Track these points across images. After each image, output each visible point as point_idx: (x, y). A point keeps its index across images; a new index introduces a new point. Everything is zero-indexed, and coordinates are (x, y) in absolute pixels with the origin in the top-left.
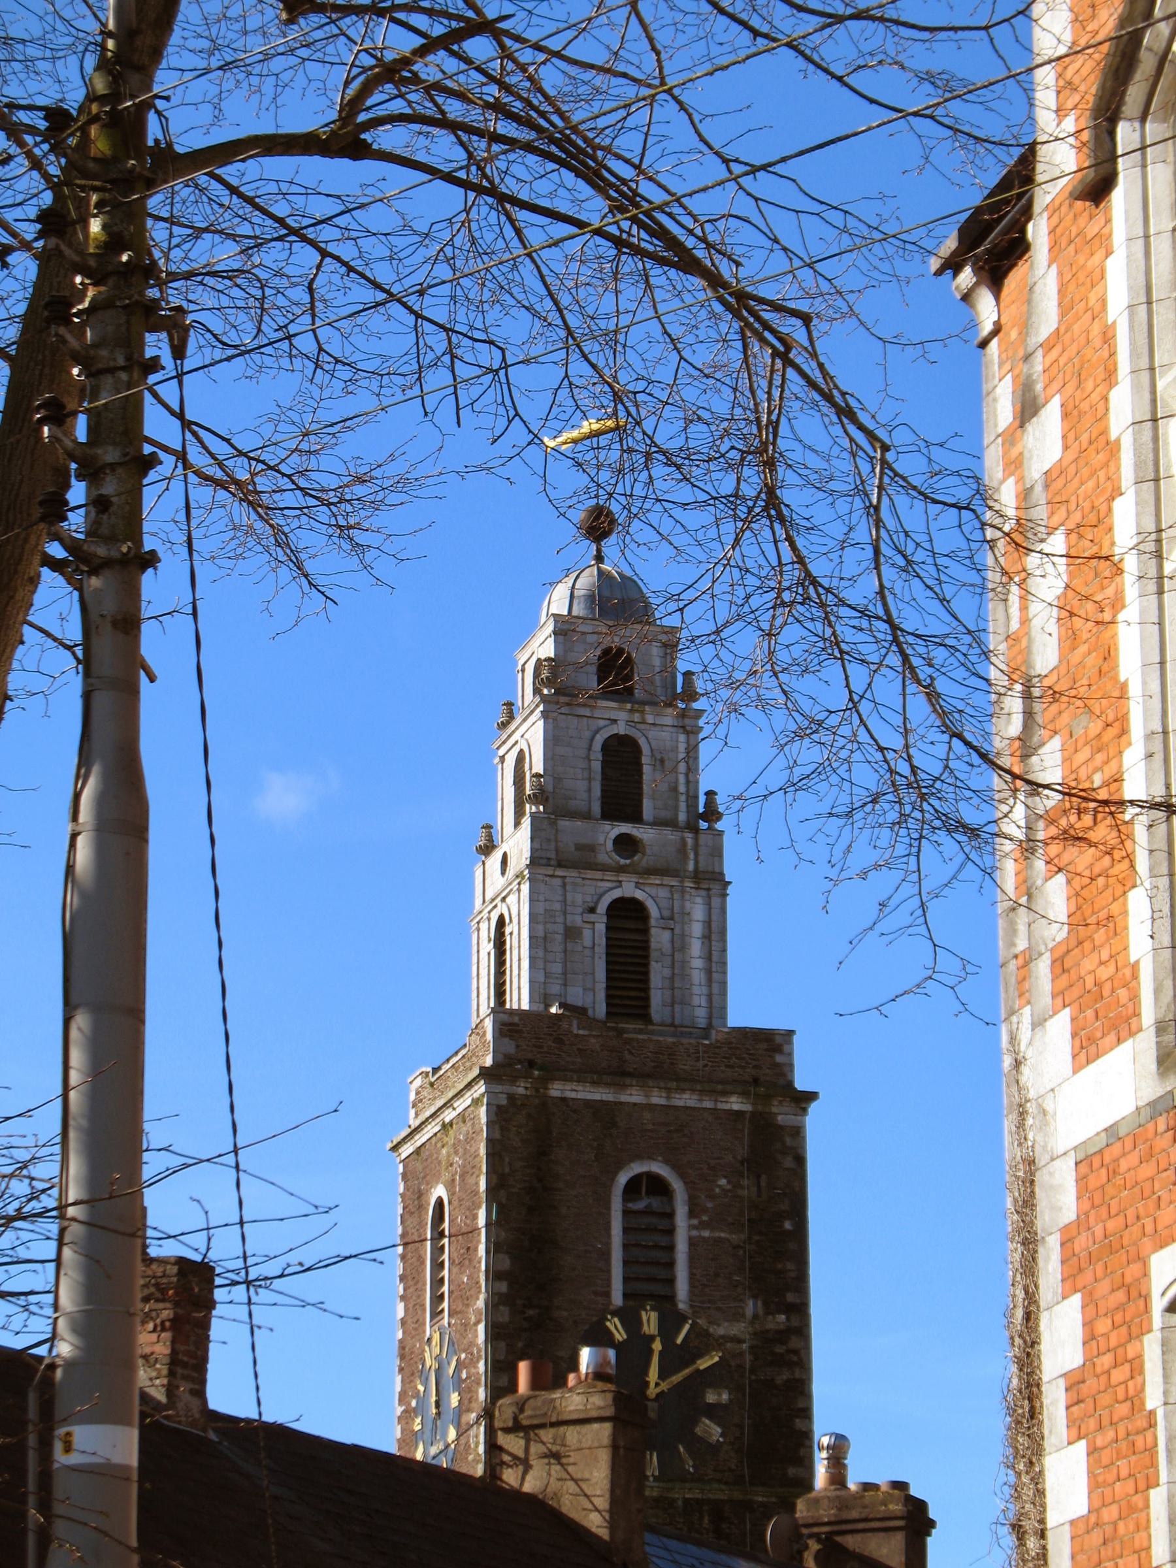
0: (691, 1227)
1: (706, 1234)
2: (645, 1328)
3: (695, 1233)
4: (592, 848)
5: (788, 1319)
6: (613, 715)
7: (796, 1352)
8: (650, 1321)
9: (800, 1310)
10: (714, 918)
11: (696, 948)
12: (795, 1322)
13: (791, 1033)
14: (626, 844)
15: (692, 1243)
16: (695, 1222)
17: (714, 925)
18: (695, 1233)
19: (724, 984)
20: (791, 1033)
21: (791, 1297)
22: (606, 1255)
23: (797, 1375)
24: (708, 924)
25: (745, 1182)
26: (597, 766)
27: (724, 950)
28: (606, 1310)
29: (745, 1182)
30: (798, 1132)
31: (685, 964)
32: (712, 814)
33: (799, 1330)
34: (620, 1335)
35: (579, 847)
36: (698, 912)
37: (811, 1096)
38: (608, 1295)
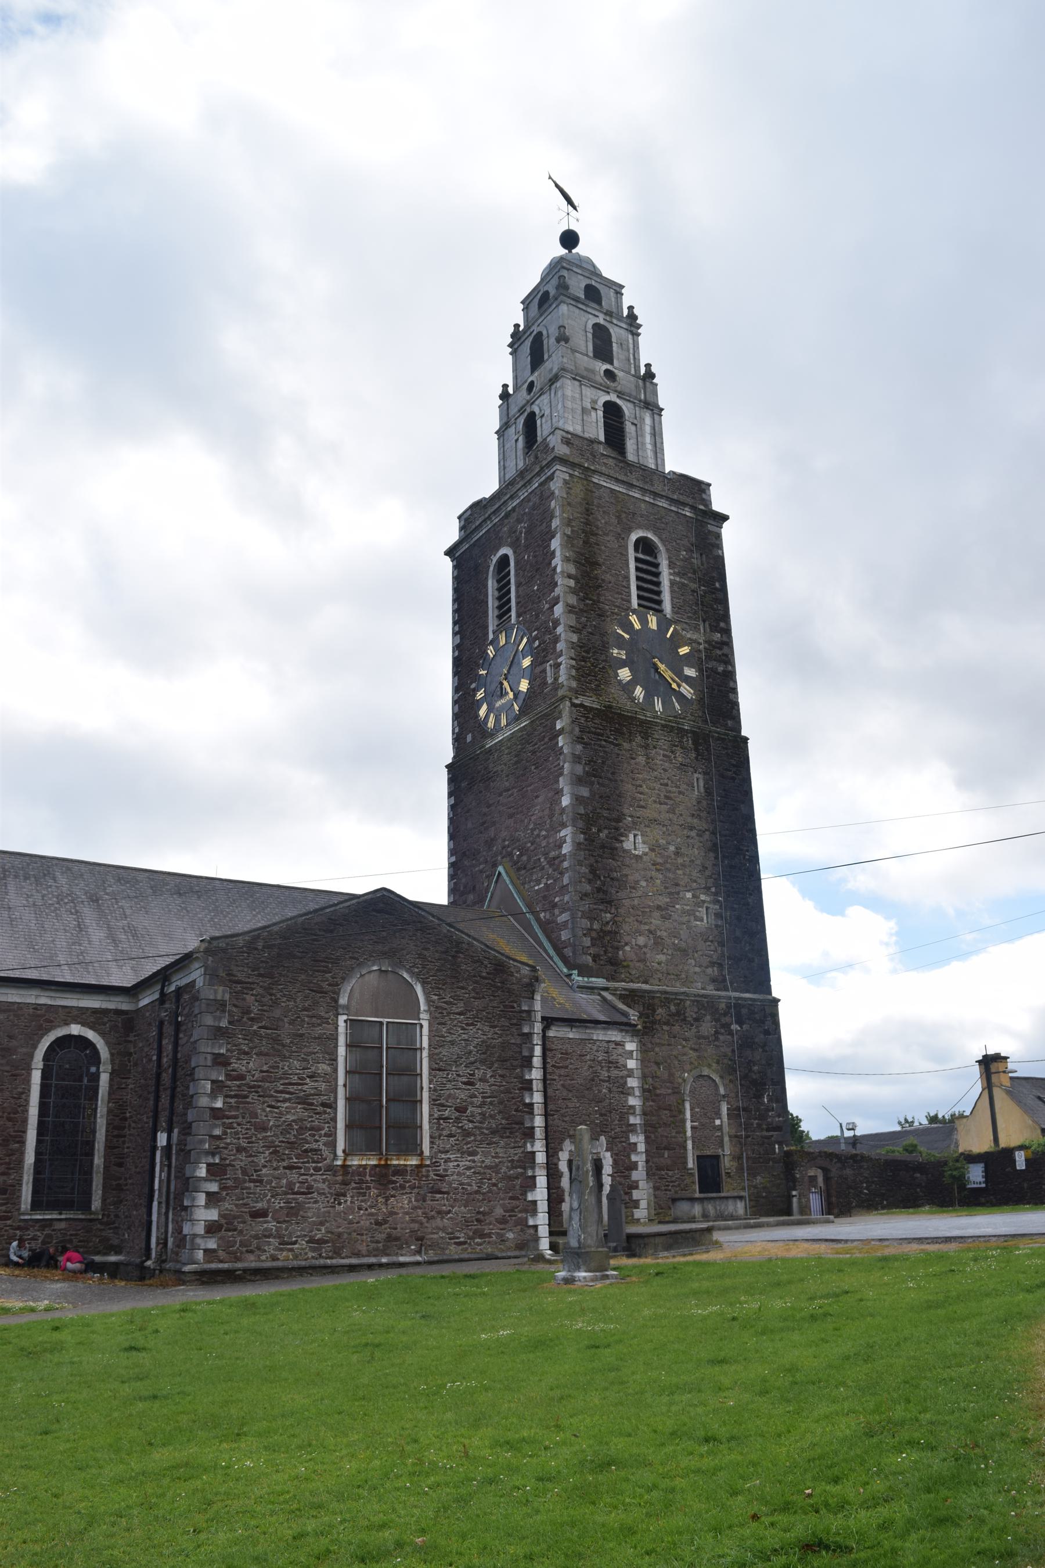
0: (670, 574)
1: (678, 579)
2: (650, 624)
3: (672, 577)
4: (593, 371)
5: (722, 636)
6: (597, 313)
7: (726, 656)
8: (653, 623)
9: (727, 631)
10: (656, 425)
11: (648, 439)
12: (725, 639)
13: (709, 485)
14: (609, 374)
15: (672, 583)
16: (672, 571)
17: (656, 428)
18: (672, 577)
19: (663, 460)
20: (709, 485)
21: (722, 625)
22: (627, 578)
23: (730, 668)
24: (653, 428)
25: (695, 555)
26: (590, 336)
27: (662, 443)
28: (629, 609)
29: (695, 555)
30: (719, 536)
31: (644, 444)
32: (650, 375)
33: (727, 643)
34: (637, 626)
35: (586, 369)
36: (648, 420)
37: (725, 518)
38: (629, 601)
